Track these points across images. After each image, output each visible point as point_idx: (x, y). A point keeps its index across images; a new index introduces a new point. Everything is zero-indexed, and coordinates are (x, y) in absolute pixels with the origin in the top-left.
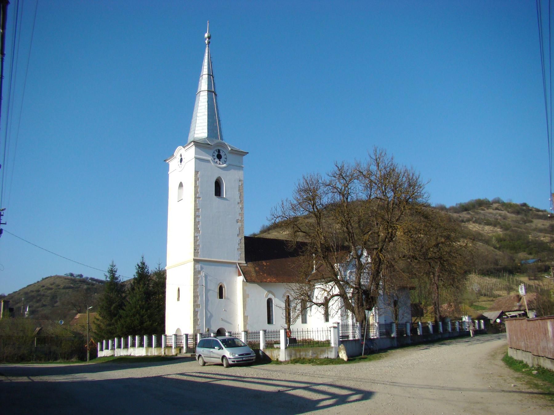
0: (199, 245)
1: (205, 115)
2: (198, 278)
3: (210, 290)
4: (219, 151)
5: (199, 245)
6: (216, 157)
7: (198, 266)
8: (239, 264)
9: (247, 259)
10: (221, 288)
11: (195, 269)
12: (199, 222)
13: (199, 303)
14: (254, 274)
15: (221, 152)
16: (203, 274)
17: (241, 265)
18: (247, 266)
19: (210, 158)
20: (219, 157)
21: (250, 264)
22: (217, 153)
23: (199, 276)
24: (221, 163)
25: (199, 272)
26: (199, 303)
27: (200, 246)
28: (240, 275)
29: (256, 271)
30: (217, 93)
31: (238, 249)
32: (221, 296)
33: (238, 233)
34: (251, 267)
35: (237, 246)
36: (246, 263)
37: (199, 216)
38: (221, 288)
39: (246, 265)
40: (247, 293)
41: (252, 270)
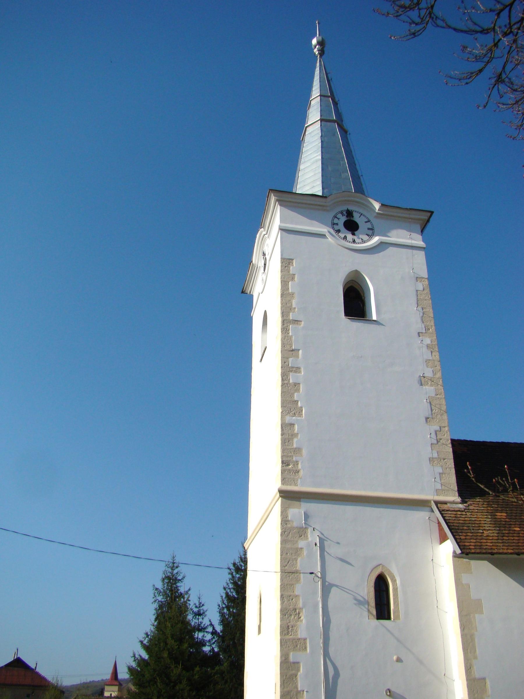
0: (298, 451)
1: (317, 161)
2: (298, 551)
3: (331, 585)
4: (349, 213)
5: (298, 451)
6: (341, 226)
7: (297, 512)
8: (437, 503)
9: (466, 489)
10: (381, 585)
11: (285, 521)
12: (296, 385)
13: (302, 632)
14: (489, 531)
15: (355, 214)
16: (313, 537)
17: (445, 507)
18: (465, 510)
19: (324, 229)
20: (352, 226)
21: (477, 504)
22: (343, 219)
23: (301, 544)
24: (357, 240)
25: (302, 532)
26: (302, 632)
27: (304, 452)
28: (443, 539)
29: (496, 522)
30: (347, 125)
31: (431, 460)
32: (383, 610)
33: (427, 413)
34: (478, 510)
35: (427, 452)
36: (463, 502)
37: (297, 370)
38: (381, 585)
39: (461, 506)
40: (474, 595)
41: (486, 521)
